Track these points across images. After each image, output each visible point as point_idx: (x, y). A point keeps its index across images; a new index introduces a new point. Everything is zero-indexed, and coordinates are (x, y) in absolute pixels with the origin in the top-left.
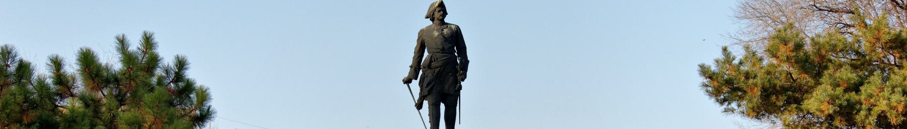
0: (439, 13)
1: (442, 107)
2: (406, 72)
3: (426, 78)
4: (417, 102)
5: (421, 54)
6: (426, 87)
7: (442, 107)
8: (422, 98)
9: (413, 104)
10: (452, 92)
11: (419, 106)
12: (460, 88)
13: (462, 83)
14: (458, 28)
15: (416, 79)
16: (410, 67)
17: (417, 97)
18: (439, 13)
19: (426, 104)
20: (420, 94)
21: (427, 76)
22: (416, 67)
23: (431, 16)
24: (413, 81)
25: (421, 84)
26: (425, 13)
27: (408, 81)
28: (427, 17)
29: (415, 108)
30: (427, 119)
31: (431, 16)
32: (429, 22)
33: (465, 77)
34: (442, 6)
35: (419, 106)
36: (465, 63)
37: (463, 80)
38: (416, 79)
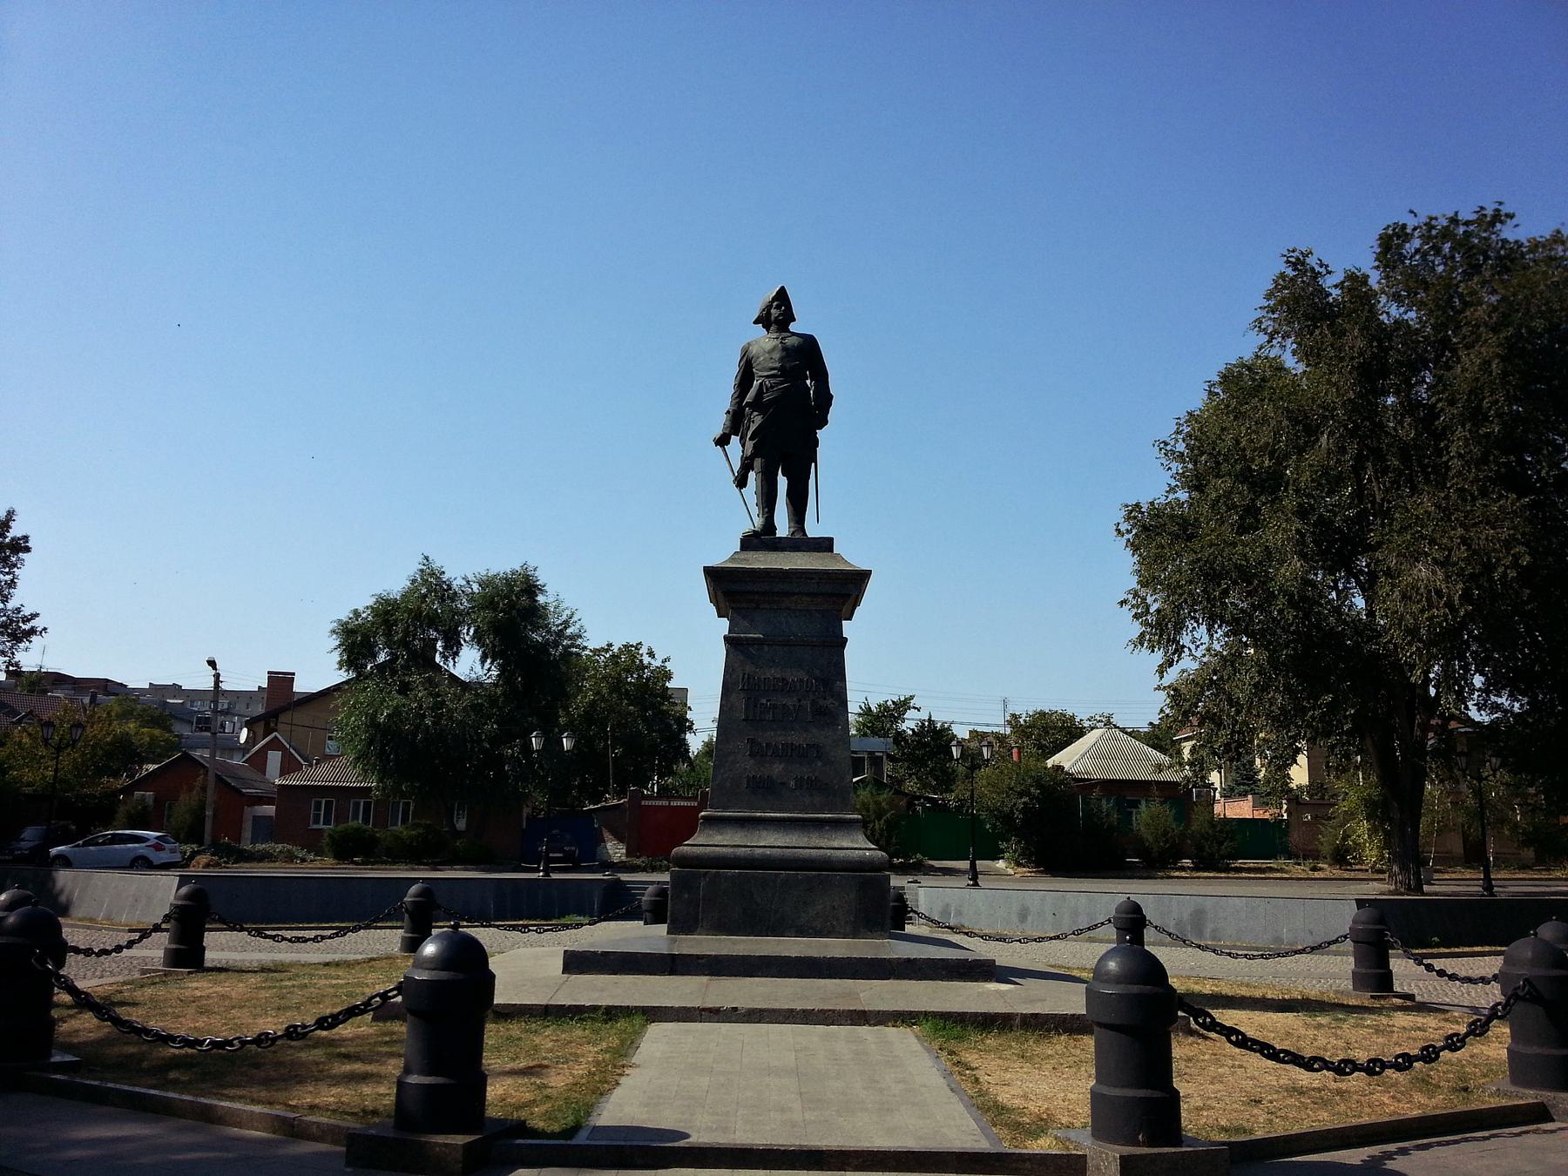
0: (778, 313)
1: (782, 483)
2: (719, 424)
4: (736, 474)
7: (782, 483)
8: (747, 466)
9: (729, 479)
11: (741, 482)
12: (816, 443)
17: (737, 465)
18: (778, 313)
19: (752, 475)
21: (753, 422)
22: (736, 422)
23: (764, 320)
27: (722, 441)
31: (764, 320)
34: (782, 296)
35: (741, 482)
36: (825, 399)
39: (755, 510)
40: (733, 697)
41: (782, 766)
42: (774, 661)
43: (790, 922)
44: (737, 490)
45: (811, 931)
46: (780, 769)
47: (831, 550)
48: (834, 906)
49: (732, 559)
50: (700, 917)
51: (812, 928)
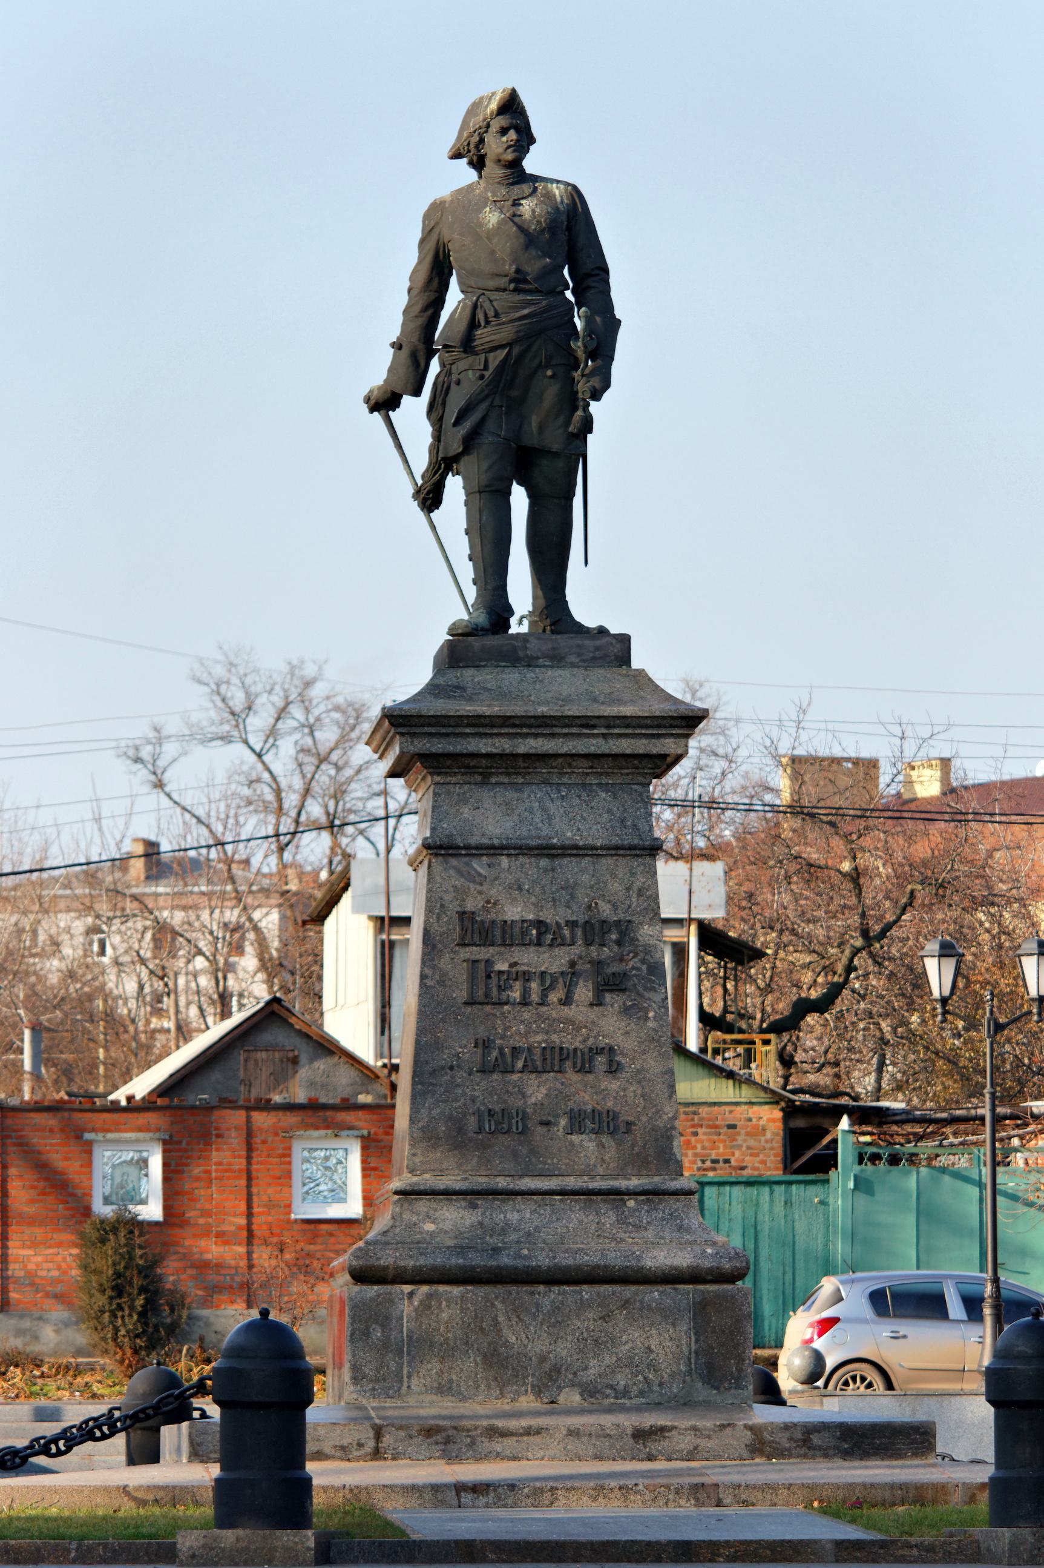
1: (519, 499)
3: (453, 386)
4: (420, 482)
5: (433, 296)
6: (456, 424)
7: (519, 499)
10: (554, 441)
12: (588, 425)
13: (594, 407)
14: (576, 195)
15: (417, 393)
16: (393, 345)
17: (421, 462)
19: (454, 487)
20: (434, 449)
21: (458, 383)
24: (407, 400)
25: (435, 410)
26: (449, 139)
28: (456, 155)
29: (414, 506)
30: (460, 546)
32: (464, 174)
33: (607, 385)
37: (597, 395)
38: (417, 393)
39: (466, 571)
40: (445, 962)
41: (543, 1090)
42: (520, 889)
43: (570, 1376)
44: (420, 515)
45: (608, 1391)
46: (540, 1096)
47: (624, 659)
48: (649, 1348)
49: (433, 689)
50: (405, 1372)
51: (611, 1387)
